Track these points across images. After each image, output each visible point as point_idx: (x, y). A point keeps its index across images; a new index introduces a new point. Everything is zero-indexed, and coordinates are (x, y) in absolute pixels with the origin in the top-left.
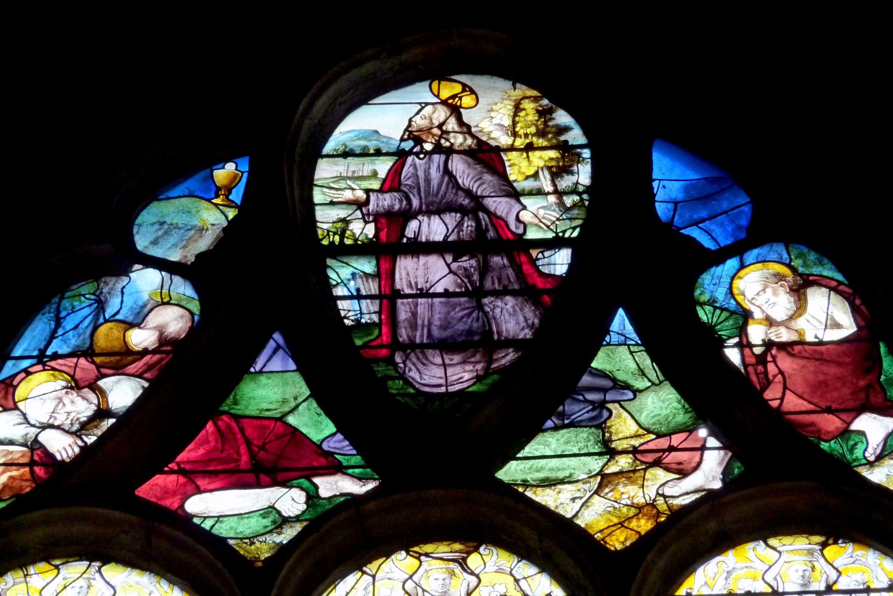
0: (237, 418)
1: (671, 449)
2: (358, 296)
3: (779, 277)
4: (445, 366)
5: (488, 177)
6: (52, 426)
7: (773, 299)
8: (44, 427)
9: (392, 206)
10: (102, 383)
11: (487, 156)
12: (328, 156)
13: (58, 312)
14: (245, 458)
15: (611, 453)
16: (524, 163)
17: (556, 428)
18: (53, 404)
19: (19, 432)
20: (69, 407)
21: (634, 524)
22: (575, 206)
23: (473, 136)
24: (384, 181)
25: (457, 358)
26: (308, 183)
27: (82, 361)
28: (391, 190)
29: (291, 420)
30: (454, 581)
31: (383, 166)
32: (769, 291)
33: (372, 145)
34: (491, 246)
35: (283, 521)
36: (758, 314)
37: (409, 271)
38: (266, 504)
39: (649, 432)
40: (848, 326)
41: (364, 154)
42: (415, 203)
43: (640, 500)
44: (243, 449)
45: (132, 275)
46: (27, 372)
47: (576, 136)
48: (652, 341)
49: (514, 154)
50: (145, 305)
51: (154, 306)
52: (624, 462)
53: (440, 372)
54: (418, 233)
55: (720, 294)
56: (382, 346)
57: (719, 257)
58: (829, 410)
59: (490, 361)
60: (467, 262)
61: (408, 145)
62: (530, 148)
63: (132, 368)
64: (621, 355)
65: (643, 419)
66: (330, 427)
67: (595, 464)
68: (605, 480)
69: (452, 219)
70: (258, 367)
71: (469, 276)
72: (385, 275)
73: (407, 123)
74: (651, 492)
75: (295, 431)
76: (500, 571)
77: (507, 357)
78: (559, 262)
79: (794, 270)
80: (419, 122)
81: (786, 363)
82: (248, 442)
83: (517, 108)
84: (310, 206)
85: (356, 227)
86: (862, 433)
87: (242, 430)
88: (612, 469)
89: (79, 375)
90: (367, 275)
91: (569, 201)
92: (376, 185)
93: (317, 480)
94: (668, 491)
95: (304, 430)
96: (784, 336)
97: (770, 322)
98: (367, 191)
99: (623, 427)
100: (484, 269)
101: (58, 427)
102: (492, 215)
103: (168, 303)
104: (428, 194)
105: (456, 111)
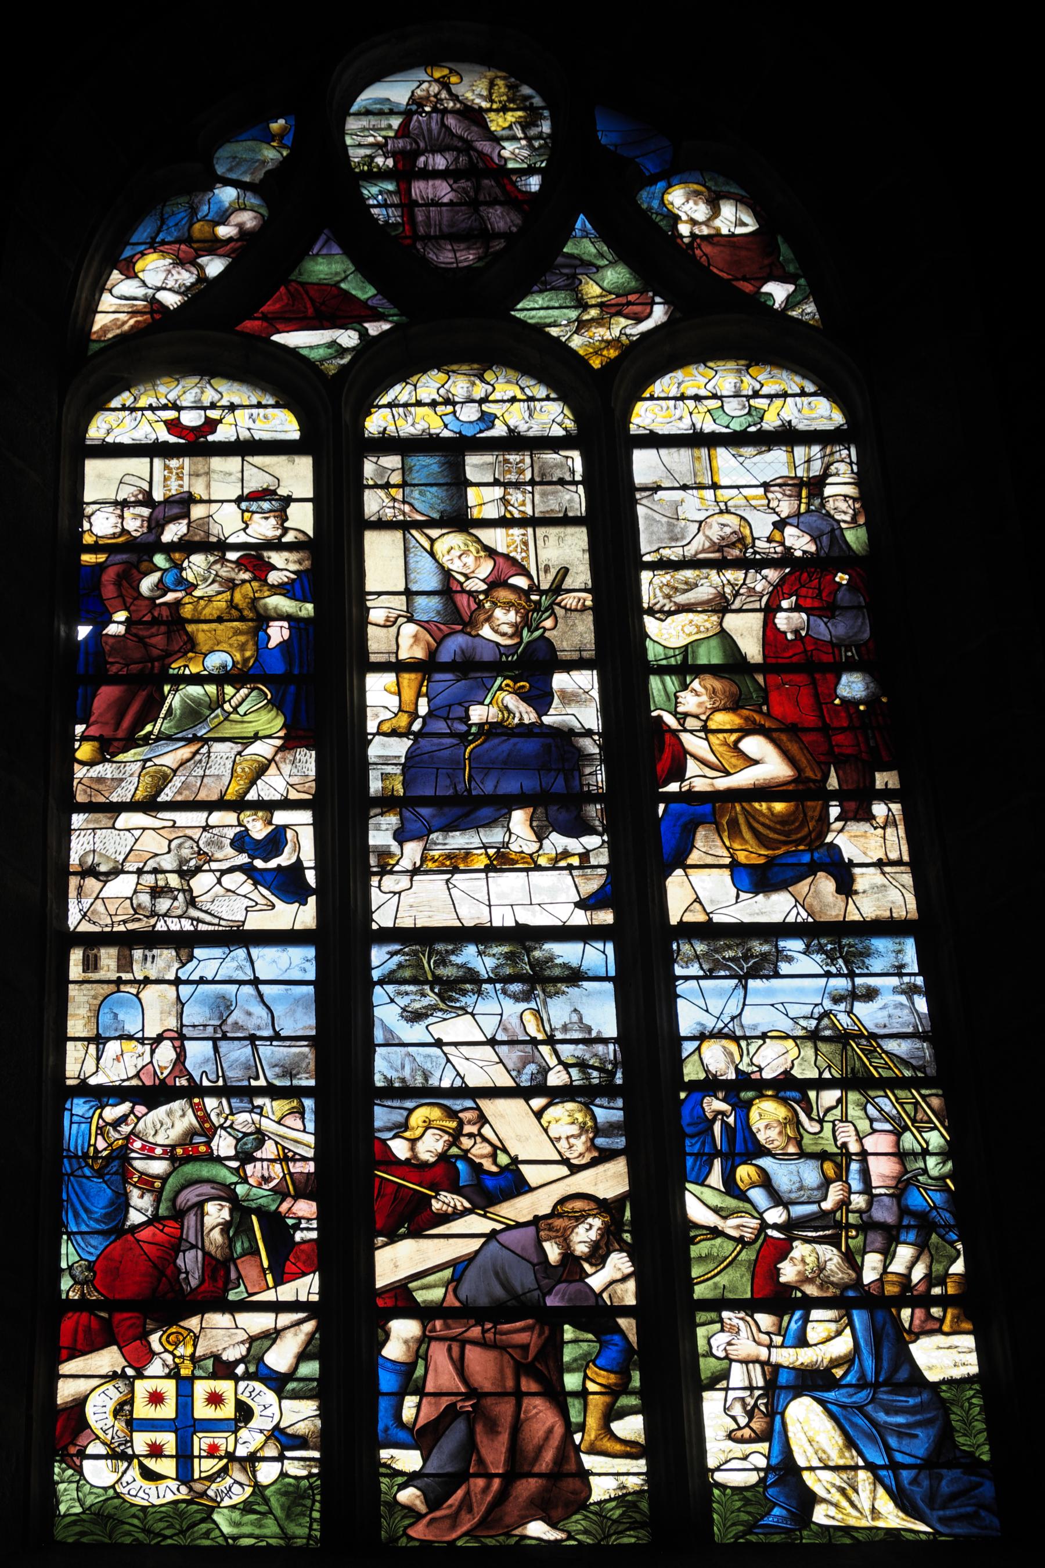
0: (303, 284)
1: (629, 303)
2: (385, 205)
3: (697, 193)
4: (454, 251)
5: (474, 128)
6: (165, 289)
7: (695, 208)
8: (158, 289)
9: (404, 147)
10: (199, 261)
11: (473, 116)
12: (354, 114)
13: (162, 214)
14: (310, 311)
15: (584, 306)
16: (500, 121)
17: (541, 291)
18: (164, 275)
19: (141, 292)
20: (176, 276)
21: (605, 353)
22: (541, 146)
23: (461, 102)
24: (397, 132)
25: (462, 246)
26: (342, 133)
27: (183, 247)
28: (403, 137)
29: (343, 285)
30: (475, 388)
31: (396, 122)
32: (691, 202)
33: (386, 108)
34: (481, 174)
35: (342, 351)
36: (684, 217)
37: (420, 189)
38: (329, 340)
39: (610, 293)
40: (751, 225)
41: (381, 113)
42: (422, 145)
43: (608, 336)
44: (309, 305)
45: (216, 191)
46: (143, 254)
47: (537, 101)
48: (605, 232)
49: (492, 115)
50: (227, 210)
51: (233, 211)
52: (594, 313)
53: (451, 255)
54: (426, 164)
55: (655, 204)
56: (407, 237)
57: (653, 181)
58: (744, 279)
59: (488, 248)
60: (463, 183)
61: (414, 107)
62: (504, 109)
63: (221, 251)
64: (584, 245)
65: (605, 285)
66: (371, 291)
67: (573, 314)
68: (581, 326)
69: (450, 156)
70: (315, 251)
71: (467, 193)
72: (403, 191)
73: (409, 94)
74: (616, 332)
75: (346, 293)
76: (508, 382)
77: (498, 245)
78: (534, 183)
79: (708, 189)
80: (419, 92)
81: (708, 249)
82: (311, 299)
83: (492, 85)
84: (345, 147)
85: (380, 161)
86: (771, 295)
87: (307, 292)
88: (586, 317)
89: (182, 255)
90: (390, 192)
91: (536, 144)
92: (391, 134)
93: (366, 325)
94: (628, 331)
95: (354, 292)
96: (705, 231)
97: (693, 222)
98: (385, 137)
99: (592, 290)
100: (478, 189)
101: (170, 290)
102: (481, 154)
103: (245, 209)
104: (430, 138)
105: (445, 85)
